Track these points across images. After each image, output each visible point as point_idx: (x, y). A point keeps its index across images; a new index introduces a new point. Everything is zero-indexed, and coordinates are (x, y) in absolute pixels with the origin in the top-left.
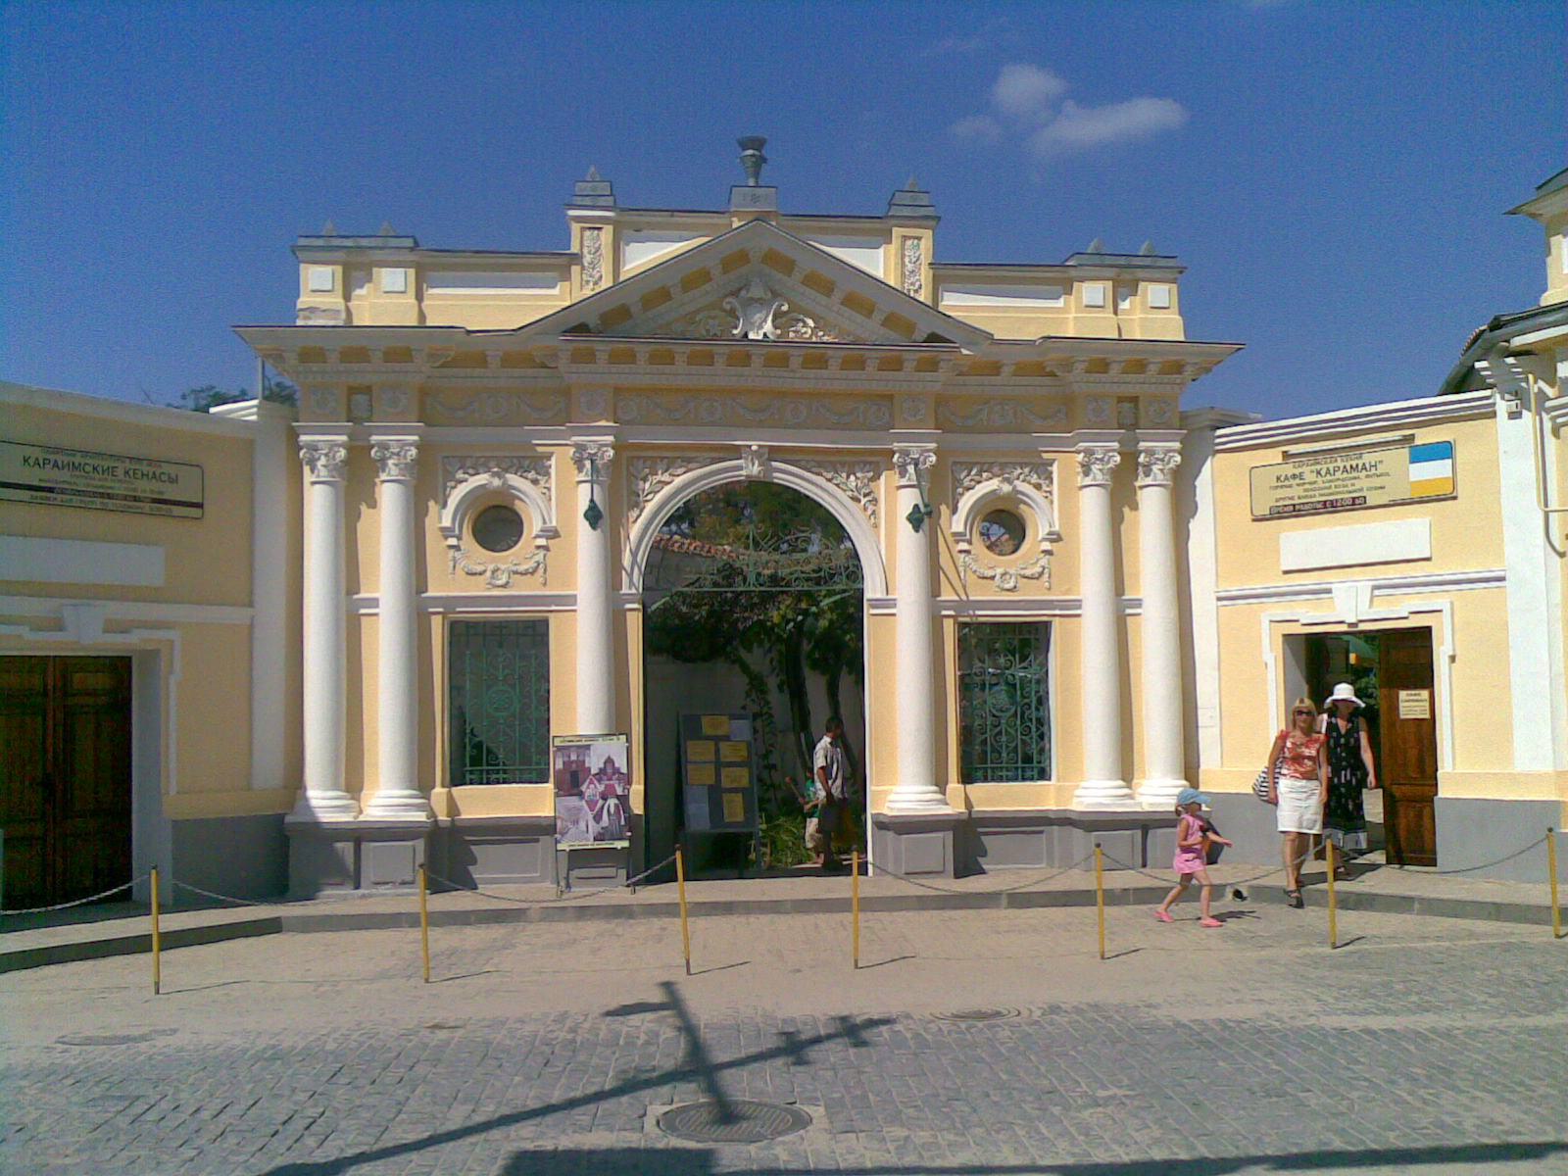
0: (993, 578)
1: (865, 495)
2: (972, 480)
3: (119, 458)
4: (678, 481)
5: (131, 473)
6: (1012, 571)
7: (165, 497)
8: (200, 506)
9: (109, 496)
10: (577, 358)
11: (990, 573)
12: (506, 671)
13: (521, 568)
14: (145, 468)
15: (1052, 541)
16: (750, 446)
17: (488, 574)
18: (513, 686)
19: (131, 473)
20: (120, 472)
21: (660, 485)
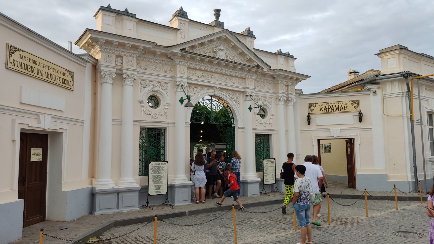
11: (261, 122)
12: (153, 143)
16: (216, 87)
17: (152, 115)
21: (194, 94)
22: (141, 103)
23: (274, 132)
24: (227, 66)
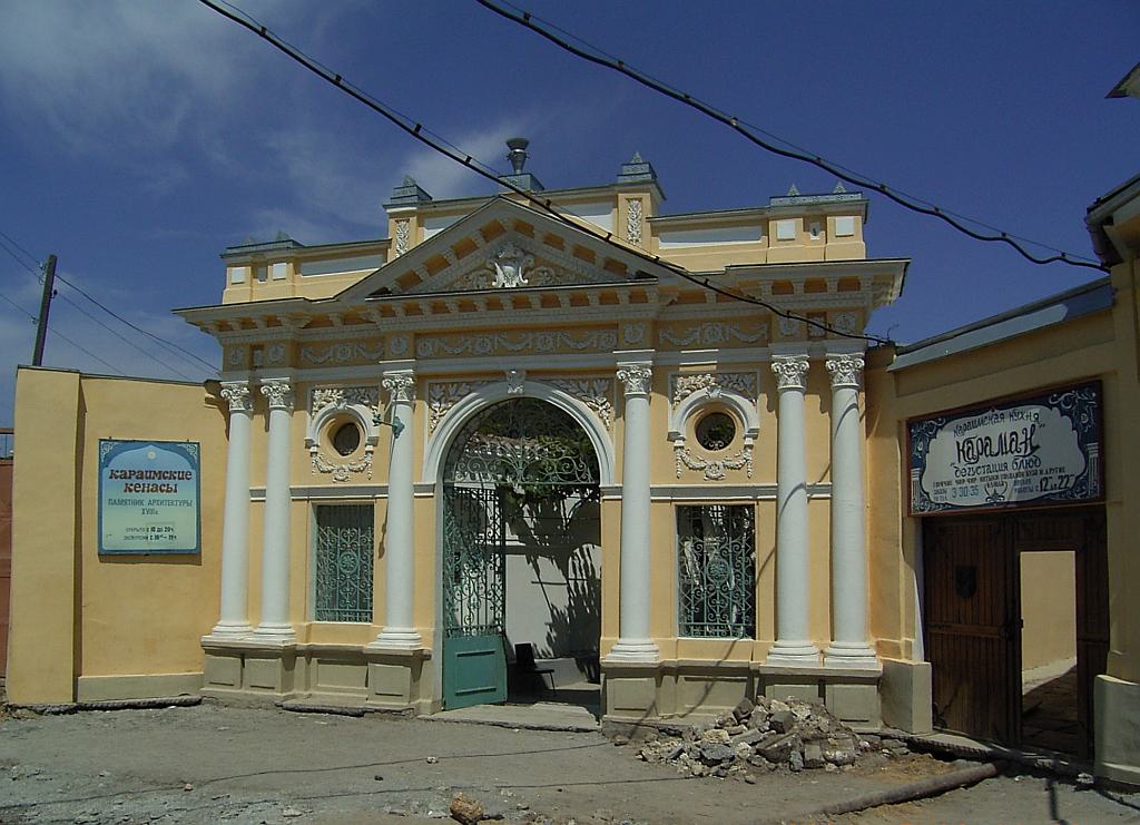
1: (602, 405)
6: (718, 463)
10: (386, 312)
13: (355, 468)
15: (755, 438)
18: (356, 552)
22: (308, 447)
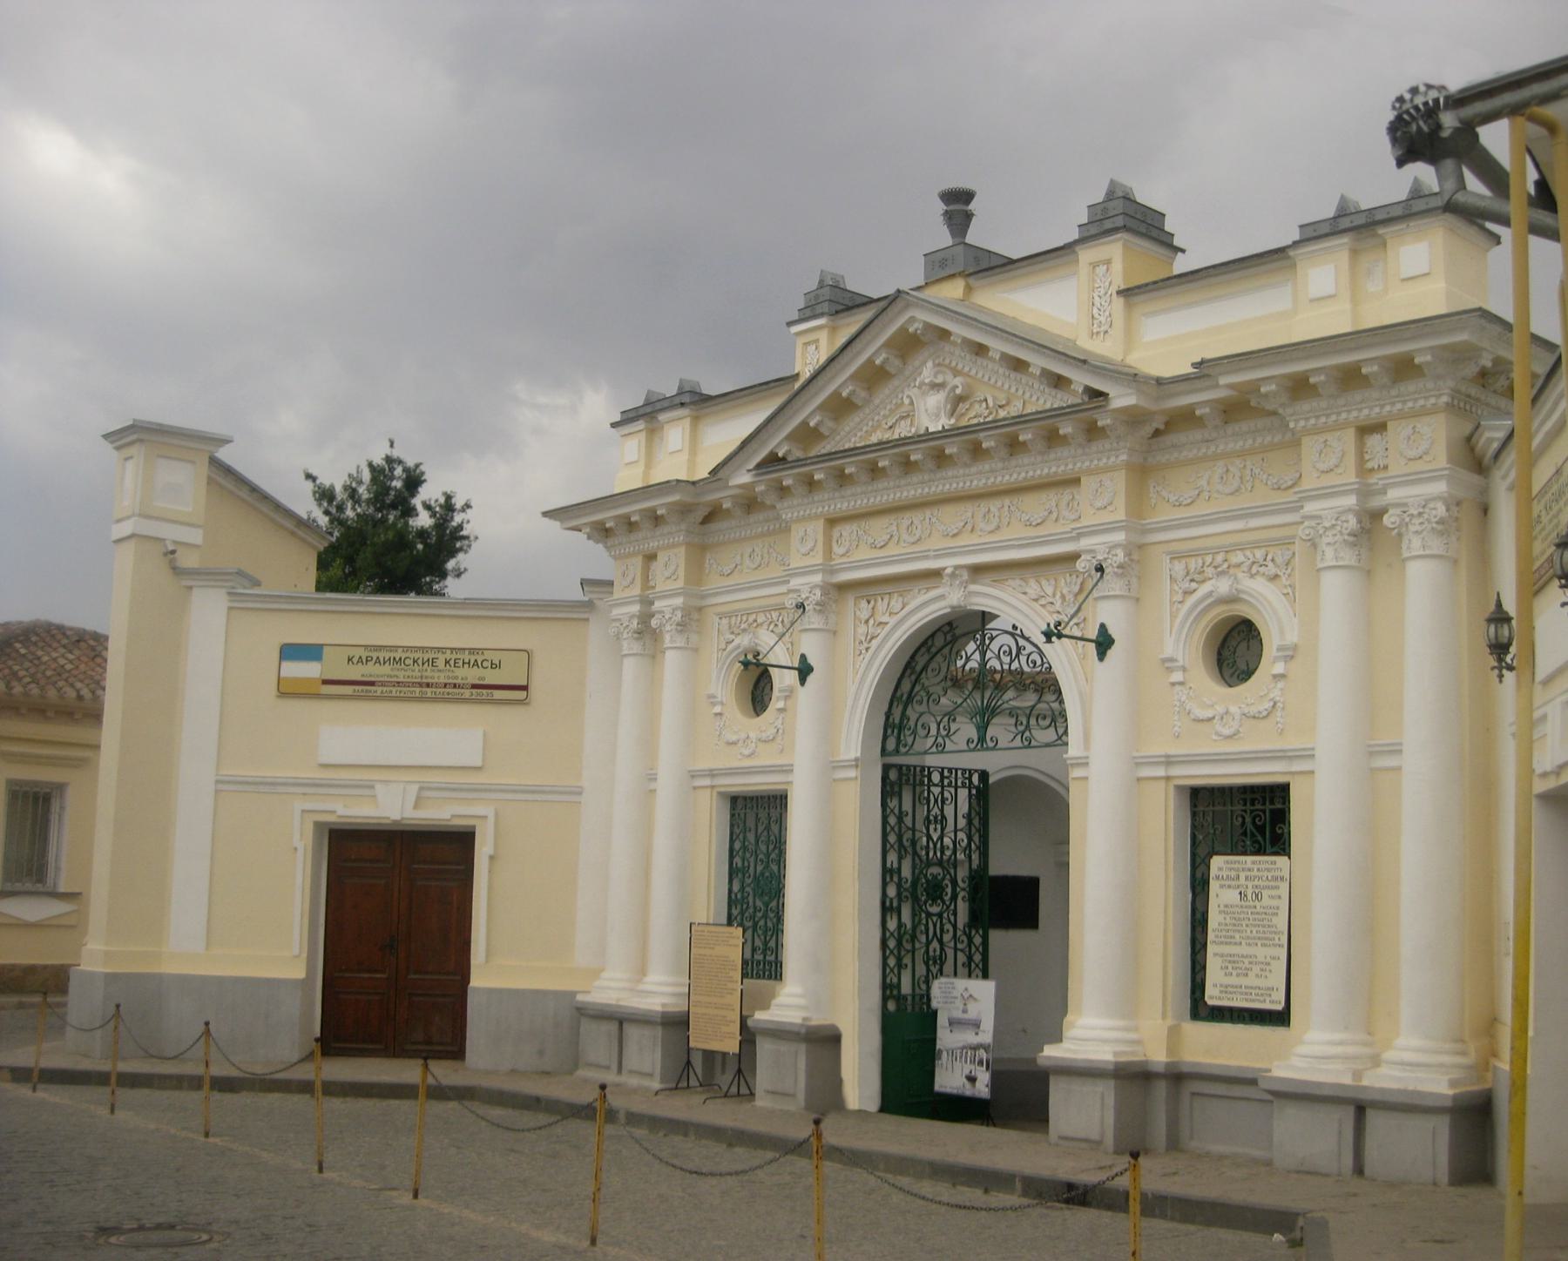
0: (1210, 719)
2: (1192, 580)
3: (439, 649)
4: (893, 621)
5: (452, 662)
6: (1233, 709)
7: (486, 682)
8: (525, 688)
9: (428, 685)
14: (466, 657)
15: (1289, 659)
19: (452, 662)
20: (441, 663)
21: (882, 626)
23: (1297, 767)
24: (977, 452)
